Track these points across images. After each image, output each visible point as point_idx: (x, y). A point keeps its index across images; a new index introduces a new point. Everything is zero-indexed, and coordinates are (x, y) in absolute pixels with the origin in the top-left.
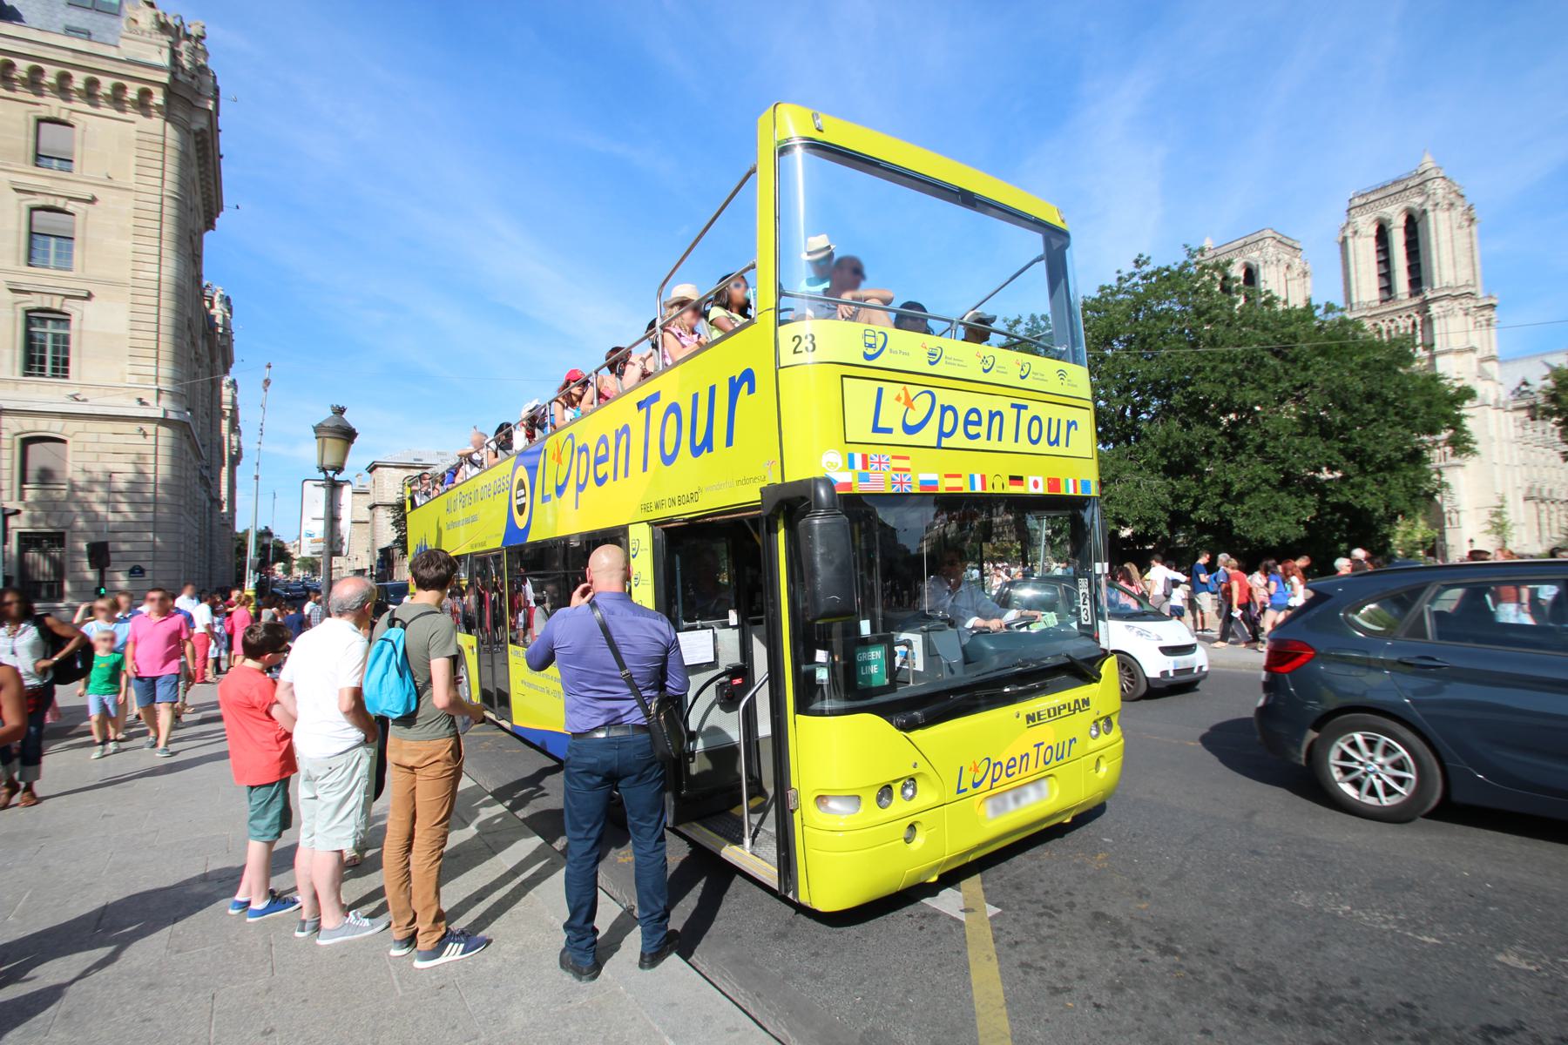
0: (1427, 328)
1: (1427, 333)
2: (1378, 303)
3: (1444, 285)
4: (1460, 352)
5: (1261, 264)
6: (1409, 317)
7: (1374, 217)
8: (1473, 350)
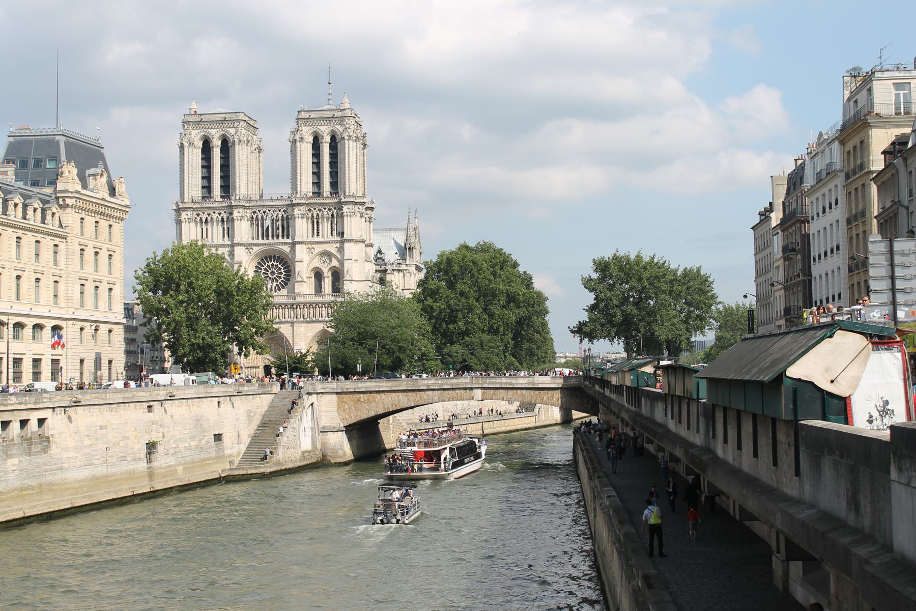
0: (340, 219)
1: (339, 224)
2: (311, 194)
3: (351, 194)
4: (357, 241)
5: (237, 142)
6: (330, 210)
7: (313, 130)
8: (363, 241)
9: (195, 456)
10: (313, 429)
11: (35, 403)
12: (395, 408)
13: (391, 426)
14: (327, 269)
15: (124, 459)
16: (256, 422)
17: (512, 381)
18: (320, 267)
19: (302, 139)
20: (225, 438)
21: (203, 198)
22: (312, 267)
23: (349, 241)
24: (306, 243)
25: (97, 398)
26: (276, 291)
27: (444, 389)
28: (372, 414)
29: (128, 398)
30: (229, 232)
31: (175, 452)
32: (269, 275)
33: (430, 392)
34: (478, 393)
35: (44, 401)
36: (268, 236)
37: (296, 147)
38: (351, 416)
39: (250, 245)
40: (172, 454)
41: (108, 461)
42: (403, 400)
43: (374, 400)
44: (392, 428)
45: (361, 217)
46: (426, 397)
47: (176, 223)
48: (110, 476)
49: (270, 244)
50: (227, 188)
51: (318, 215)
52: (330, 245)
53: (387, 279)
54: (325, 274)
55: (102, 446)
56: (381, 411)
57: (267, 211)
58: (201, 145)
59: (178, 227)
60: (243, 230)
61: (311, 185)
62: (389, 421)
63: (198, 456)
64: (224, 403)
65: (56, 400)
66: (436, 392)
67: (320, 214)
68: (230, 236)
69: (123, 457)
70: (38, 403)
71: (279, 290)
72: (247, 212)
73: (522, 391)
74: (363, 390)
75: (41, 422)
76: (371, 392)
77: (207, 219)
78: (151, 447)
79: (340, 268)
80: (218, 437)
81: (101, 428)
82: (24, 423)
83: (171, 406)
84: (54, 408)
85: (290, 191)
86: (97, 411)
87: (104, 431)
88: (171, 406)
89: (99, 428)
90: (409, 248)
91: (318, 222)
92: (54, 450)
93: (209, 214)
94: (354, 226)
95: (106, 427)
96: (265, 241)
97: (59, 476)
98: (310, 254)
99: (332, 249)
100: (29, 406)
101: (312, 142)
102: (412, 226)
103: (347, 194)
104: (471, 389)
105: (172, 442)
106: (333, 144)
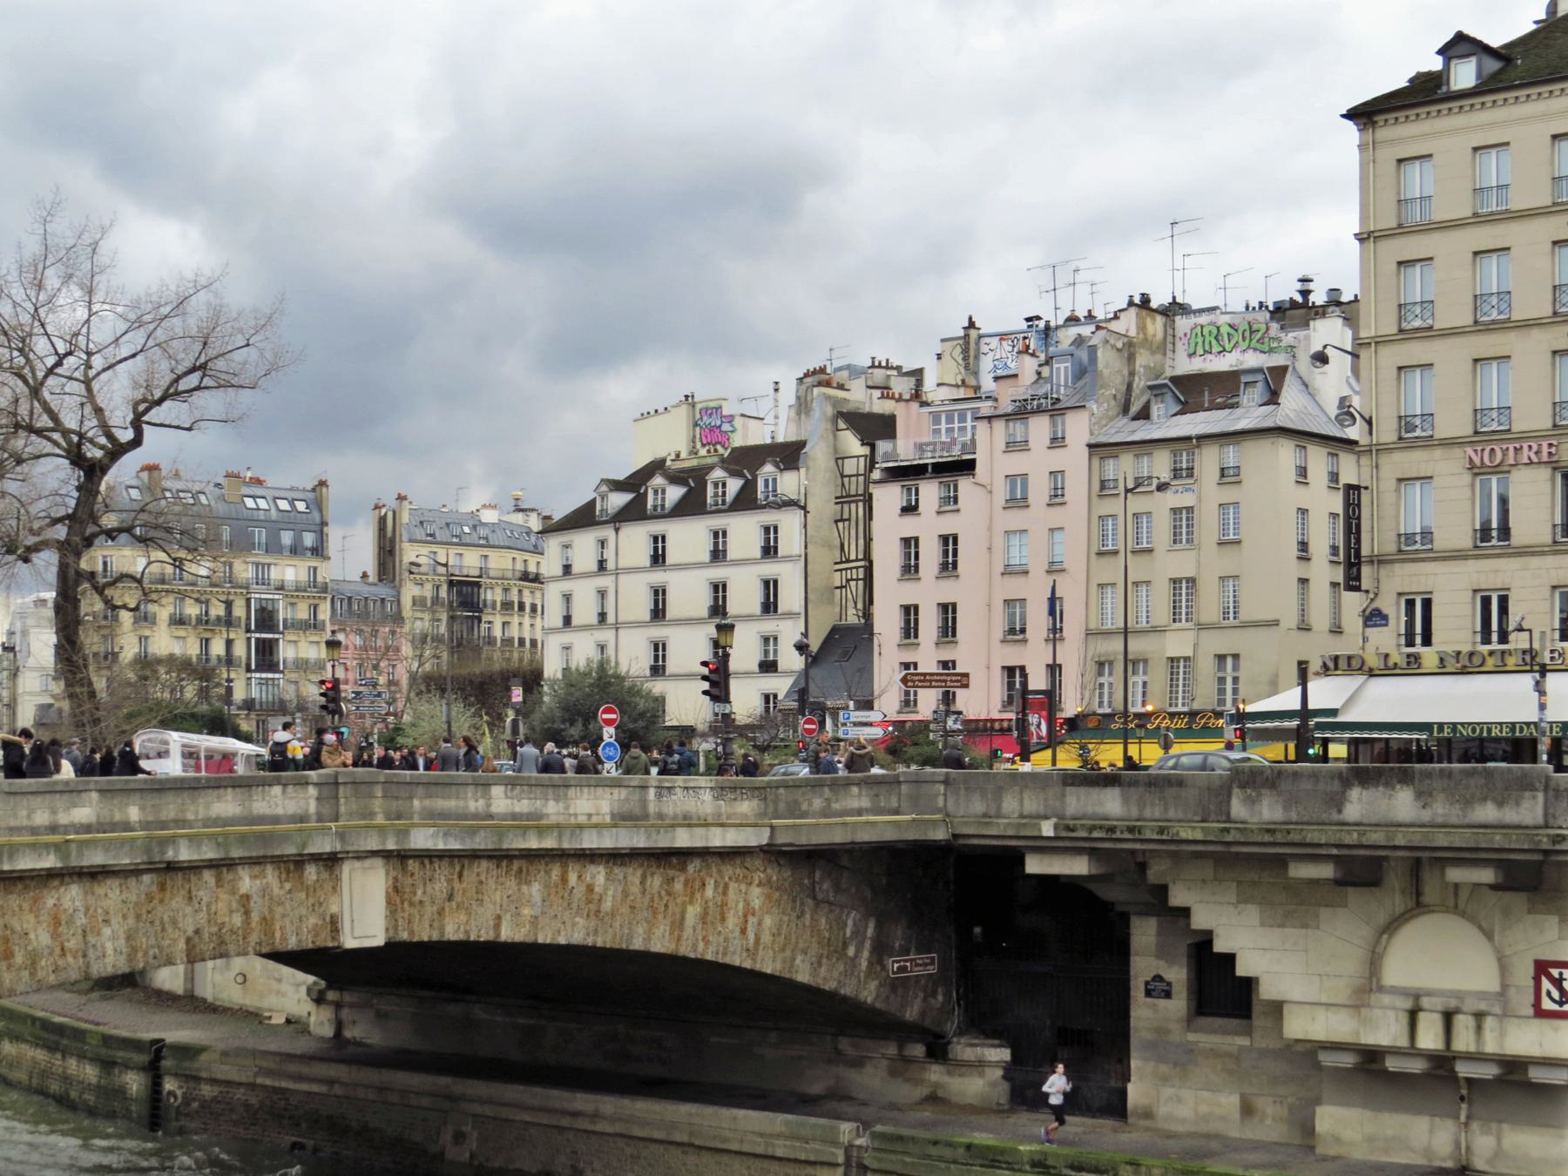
27: (172, 867)
33: (72, 896)
46: (42, 938)
66: (112, 894)
104: (331, 861)
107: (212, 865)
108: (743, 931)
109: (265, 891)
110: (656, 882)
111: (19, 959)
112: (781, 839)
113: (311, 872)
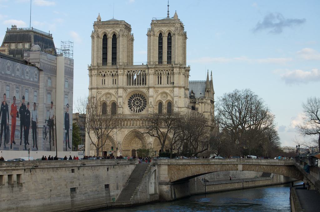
0: (172, 76)
1: (172, 78)
2: (157, 63)
4: (180, 87)
5: (121, 35)
7: (159, 30)
9: (95, 196)
10: (155, 183)
11: (15, 167)
12: (197, 174)
13: (196, 183)
14: (165, 101)
15: (58, 196)
16: (126, 179)
17: (258, 161)
18: (161, 100)
19: (154, 35)
20: (111, 187)
21: (103, 64)
22: (157, 100)
23: (176, 87)
24: (154, 88)
25: (47, 165)
26: (139, 112)
27: (223, 164)
28: (186, 176)
29: (62, 165)
30: (115, 82)
31: (85, 193)
32: (135, 102)
33: (216, 166)
34: (240, 167)
35: (20, 165)
36: (135, 84)
37: (150, 39)
38: (175, 177)
39: (126, 88)
40: (84, 194)
41: (52, 197)
42: (202, 170)
43: (187, 169)
44: (196, 184)
45: (183, 74)
46: (214, 169)
47: (89, 76)
48: (52, 204)
49: (136, 88)
50: (114, 59)
51: (161, 74)
52: (167, 89)
53: (196, 107)
54: (164, 104)
55: (48, 189)
56: (190, 175)
57: (135, 71)
58: (102, 37)
59: (90, 79)
60: (122, 80)
61: (158, 59)
62: (194, 180)
63: (97, 196)
64: (110, 169)
65: (26, 165)
66: (219, 166)
67: (162, 73)
68: (116, 84)
69: (59, 195)
70: (17, 167)
71: (141, 111)
72: (125, 71)
73: (263, 166)
74: (181, 164)
75: (19, 176)
76: (185, 165)
77: (105, 75)
78: (73, 190)
79: (171, 100)
80: (107, 186)
81: (48, 179)
82: (10, 176)
83: (84, 169)
84: (25, 169)
85: (146, 60)
86: (46, 171)
87: (50, 181)
88: (84, 169)
89: (47, 180)
90: (208, 91)
91: (161, 77)
92: (24, 190)
93: (106, 72)
94: (178, 79)
95: (50, 179)
96: (135, 86)
97: (27, 203)
98: (157, 93)
99: (167, 91)
100: (13, 168)
101: (159, 36)
102: (210, 80)
103: (176, 63)
104: (237, 164)
105: (83, 188)
106: (169, 37)
107: (226, 164)
108: (282, 172)
109: (231, 166)
110: (271, 167)
111: (212, 170)
112: (285, 164)
113: (235, 165)
